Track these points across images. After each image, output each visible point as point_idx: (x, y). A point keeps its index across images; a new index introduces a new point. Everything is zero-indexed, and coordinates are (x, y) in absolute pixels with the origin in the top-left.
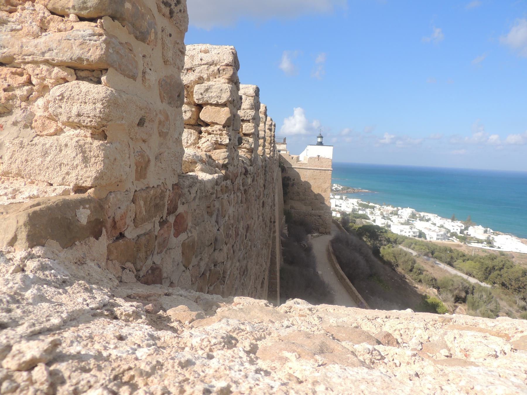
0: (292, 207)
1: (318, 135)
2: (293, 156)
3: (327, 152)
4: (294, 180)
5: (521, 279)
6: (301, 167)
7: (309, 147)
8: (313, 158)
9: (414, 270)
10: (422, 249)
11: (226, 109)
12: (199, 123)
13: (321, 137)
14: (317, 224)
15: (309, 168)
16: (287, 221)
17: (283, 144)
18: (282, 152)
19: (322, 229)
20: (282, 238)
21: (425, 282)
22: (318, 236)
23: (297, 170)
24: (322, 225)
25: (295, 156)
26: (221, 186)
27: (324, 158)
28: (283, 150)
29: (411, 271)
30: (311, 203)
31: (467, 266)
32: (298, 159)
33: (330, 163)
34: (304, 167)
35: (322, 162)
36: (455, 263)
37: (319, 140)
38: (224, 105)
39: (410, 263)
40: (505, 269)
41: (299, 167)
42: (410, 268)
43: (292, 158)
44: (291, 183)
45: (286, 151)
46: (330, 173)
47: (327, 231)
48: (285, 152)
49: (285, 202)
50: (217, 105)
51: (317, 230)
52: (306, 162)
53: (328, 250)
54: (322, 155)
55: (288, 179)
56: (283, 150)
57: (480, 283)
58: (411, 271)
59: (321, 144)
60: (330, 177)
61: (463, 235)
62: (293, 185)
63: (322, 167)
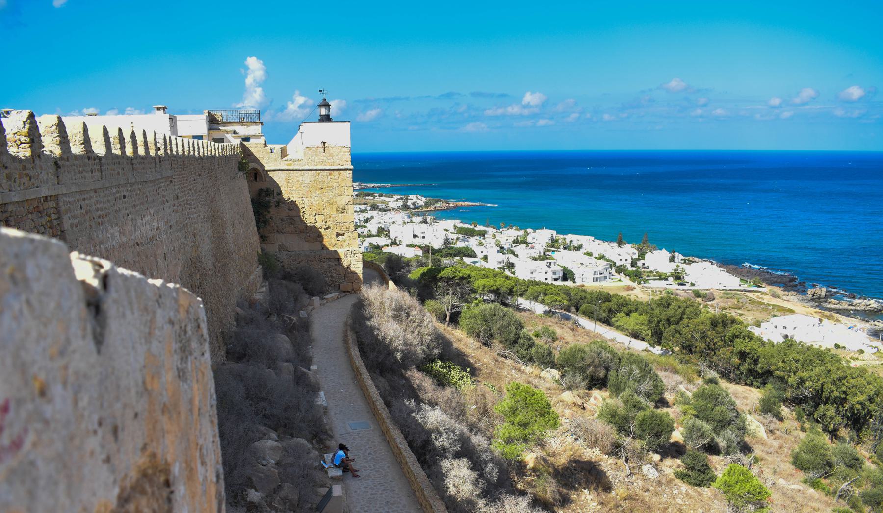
0: (282, 248)
1: (320, 101)
3: (339, 135)
5: (709, 333)
6: (291, 168)
7: (305, 127)
9: (521, 341)
10: (556, 301)
16: (265, 277)
17: (255, 123)
20: (238, 309)
21: (538, 359)
22: (338, 298)
28: (255, 136)
29: (515, 342)
31: (632, 321)
35: (331, 155)
36: (614, 319)
37: (323, 111)
39: (513, 328)
40: (686, 321)
42: (512, 336)
44: (273, 200)
46: (349, 174)
49: (263, 238)
51: (337, 287)
53: (346, 324)
57: (651, 349)
58: (515, 342)
59: (327, 119)
61: (96, 259)
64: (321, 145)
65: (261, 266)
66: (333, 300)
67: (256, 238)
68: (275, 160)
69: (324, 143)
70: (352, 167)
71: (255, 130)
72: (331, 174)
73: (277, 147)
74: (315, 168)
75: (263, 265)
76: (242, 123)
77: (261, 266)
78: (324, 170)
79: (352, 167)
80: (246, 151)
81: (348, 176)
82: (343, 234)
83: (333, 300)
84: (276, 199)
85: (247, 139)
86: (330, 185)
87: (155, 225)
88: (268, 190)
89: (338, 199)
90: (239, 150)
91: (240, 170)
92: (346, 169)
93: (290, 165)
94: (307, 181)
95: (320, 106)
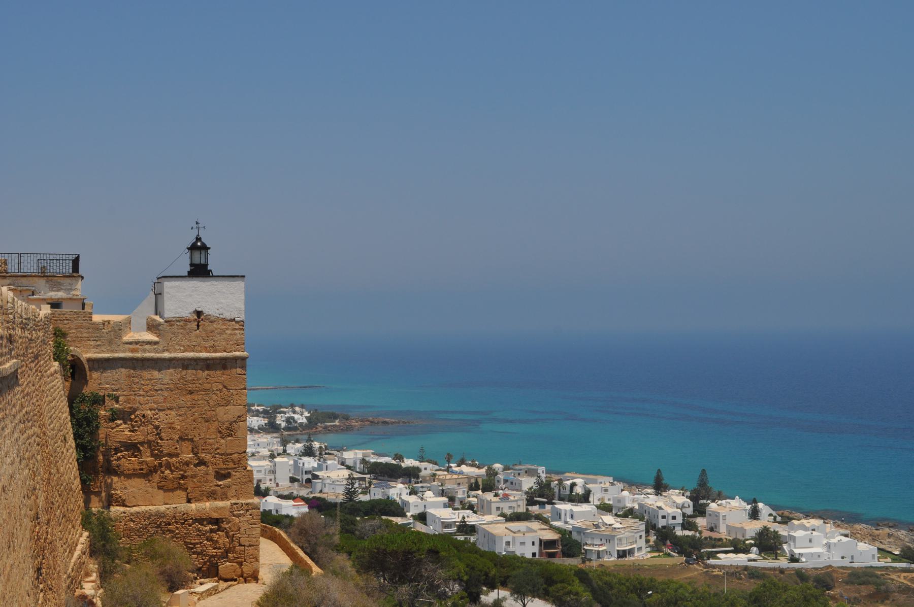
8: (180, 319)
16: (93, 551)
47: (247, 569)
51: (210, 571)
54: (210, 309)
65: (86, 534)
66: (209, 593)
69: (199, 313)
75: (91, 530)
77: (86, 534)
82: (228, 476)
83: (209, 593)
86: (208, 386)
87: (50, 447)
89: (220, 411)
91: (55, 360)
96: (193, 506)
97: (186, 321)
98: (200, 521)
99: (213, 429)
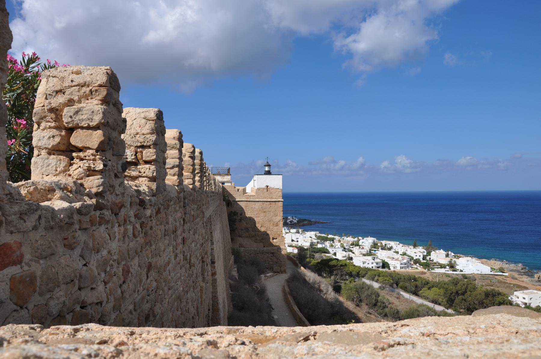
0: (241, 246)
1: (265, 163)
2: (238, 188)
3: (276, 182)
4: (241, 215)
5: (485, 301)
6: (249, 200)
7: (256, 177)
8: (261, 188)
9: (379, 304)
10: (386, 280)
11: (100, 132)
12: (72, 149)
13: (269, 166)
14: (271, 263)
15: (257, 200)
16: (236, 262)
17: (227, 175)
18: (226, 184)
19: (276, 268)
20: (230, 281)
21: (391, 315)
22: (273, 276)
23: (242, 204)
24: (276, 263)
25: (241, 188)
26: (91, 217)
27: (273, 188)
28: (228, 182)
29: (375, 305)
30: (262, 239)
31: (432, 293)
32: (244, 191)
33: (281, 194)
34: (251, 200)
35: (271, 193)
36: (421, 292)
37: (267, 169)
38: (96, 128)
39: (374, 296)
40: (469, 293)
41: (246, 200)
42: (374, 302)
43: (238, 190)
45: (231, 182)
46: (281, 204)
47: (282, 269)
48: (230, 184)
49: (232, 240)
50: (89, 128)
51: (271, 269)
52: (254, 194)
53: (284, 291)
54: (271, 185)
55: (235, 214)
56: (228, 182)
57: (446, 310)
58: (375, 305)
59: (268, 173)
60: (281, 209)
62: (241, 220)
63: (272, 198)
64: (266, 188)
66: (271, 276)
67: (230, 240)
68: (240, 195)
69: (268, 186)
70: (282, 200)
71: (227, 178)
72: (270, 204)
73: (241, 188)
74: (262, 200)
75: (235, 255)
76: (219, 174)
78: (267, 202)
79: (282, 200)
80: (224, 189)
81: (280, 205)
82: (276, 239)
83: (271, 276)
84: (239, 218)
85: (223, 183)
88: (235, 212)
90: (221, 190)
92: (279, 201)
93: (248, 198)
94: (257, 207)
95: (265, 166)
96: (265, 248)
97: (264, 189)
98: (268, 253)
99: (272, 224)
